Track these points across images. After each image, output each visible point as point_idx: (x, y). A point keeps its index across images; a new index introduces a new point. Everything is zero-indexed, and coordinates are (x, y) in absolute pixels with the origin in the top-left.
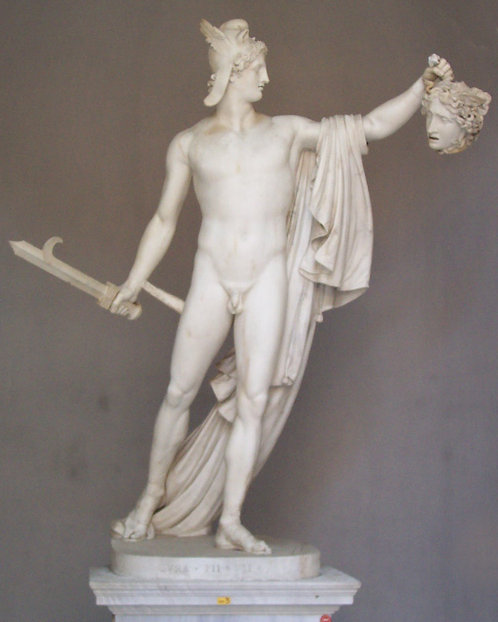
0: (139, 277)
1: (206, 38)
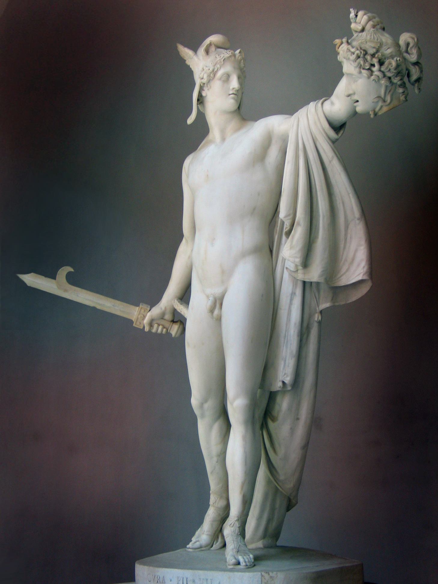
0: (169, 296)
1: (185, 61)
